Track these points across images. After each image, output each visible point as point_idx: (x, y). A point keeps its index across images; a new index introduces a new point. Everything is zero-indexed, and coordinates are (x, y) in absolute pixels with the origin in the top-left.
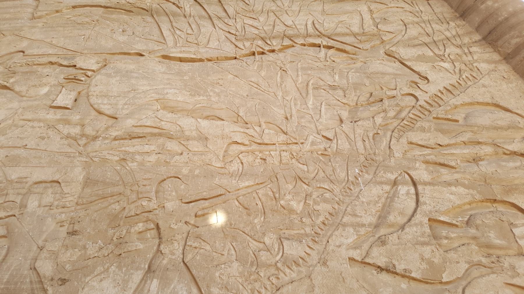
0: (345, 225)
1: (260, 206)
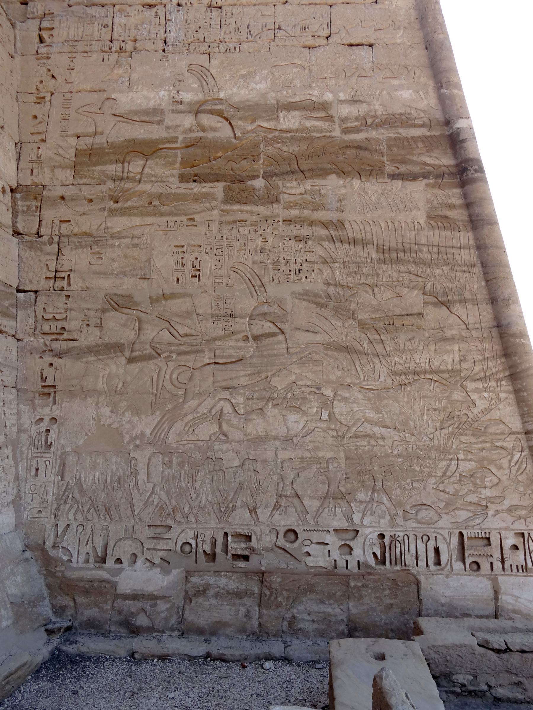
0: (432, 476)
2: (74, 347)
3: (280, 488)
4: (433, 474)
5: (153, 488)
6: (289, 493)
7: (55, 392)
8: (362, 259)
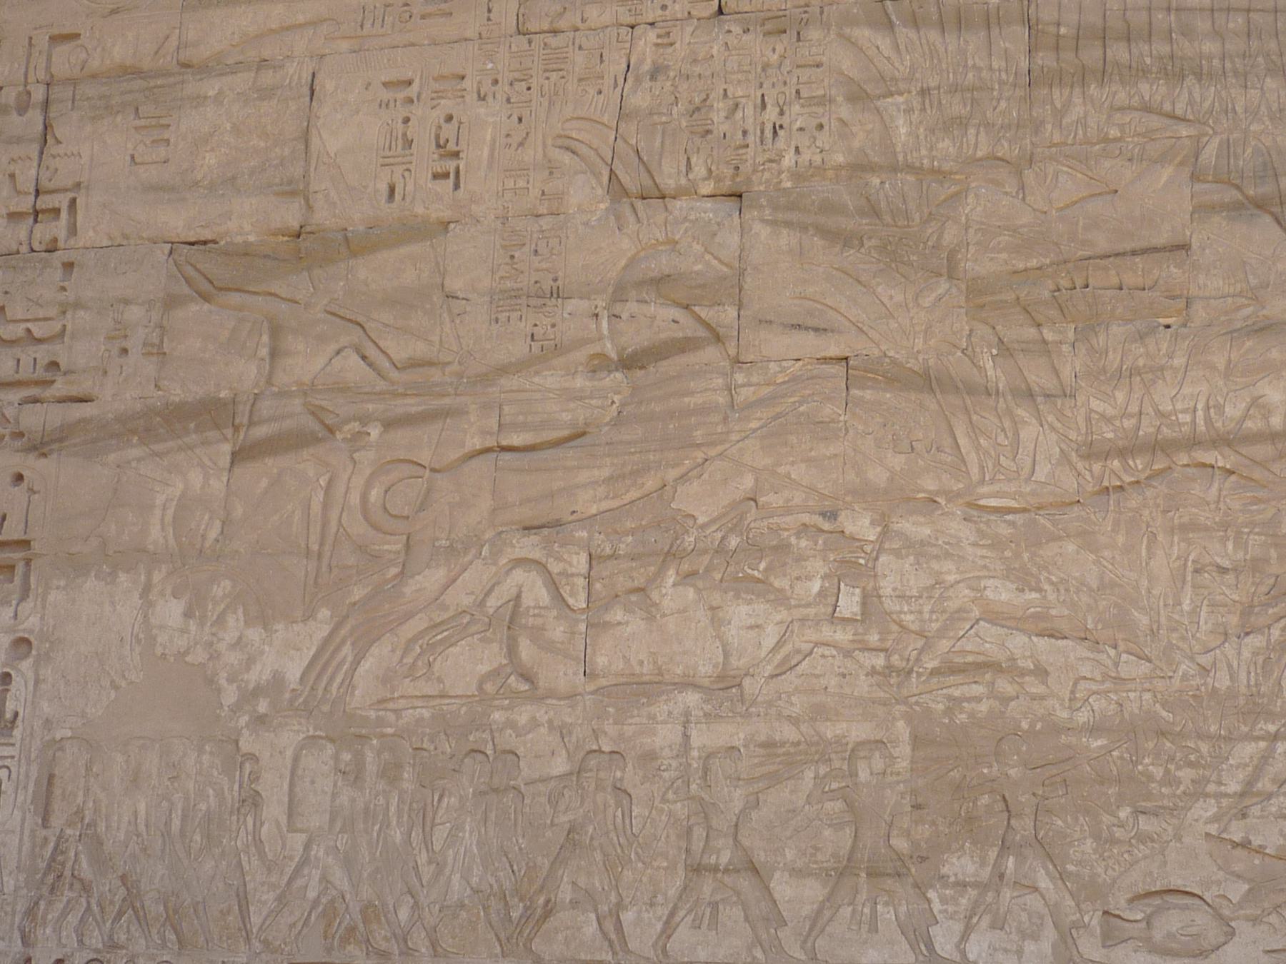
0: (1207, 795)
1: (1115, 773)
2: (83, 421)
3: (697, 845)
4: (1211, 788)
5: (307, 847)
6: (724, 859)
7: (28, 562)
8: (984, 74)
